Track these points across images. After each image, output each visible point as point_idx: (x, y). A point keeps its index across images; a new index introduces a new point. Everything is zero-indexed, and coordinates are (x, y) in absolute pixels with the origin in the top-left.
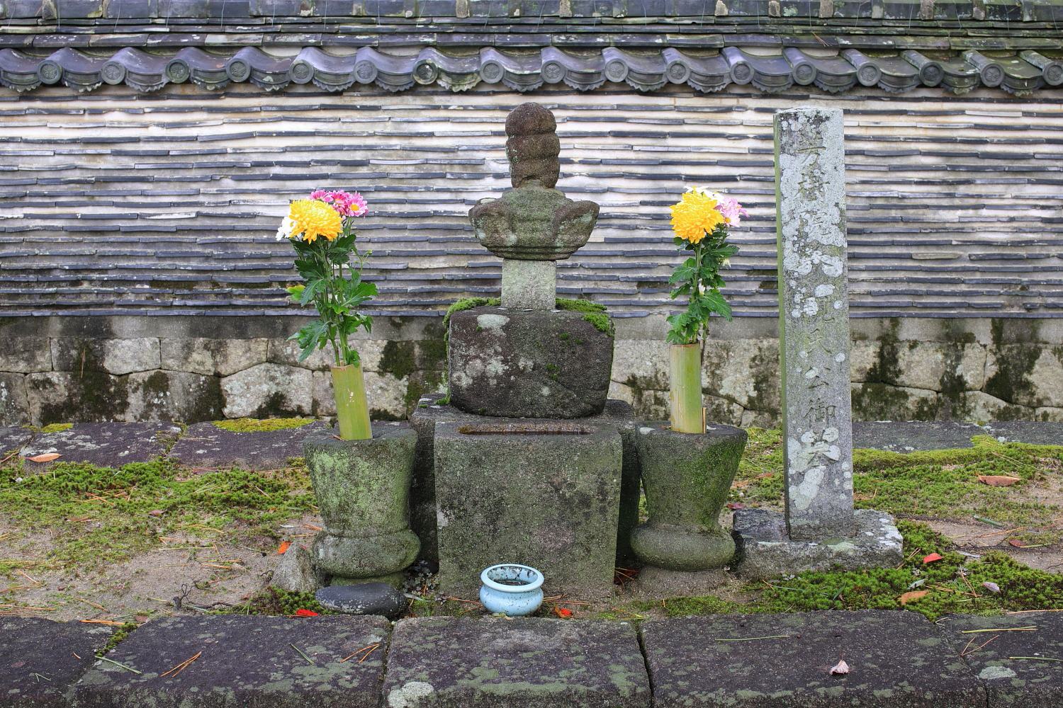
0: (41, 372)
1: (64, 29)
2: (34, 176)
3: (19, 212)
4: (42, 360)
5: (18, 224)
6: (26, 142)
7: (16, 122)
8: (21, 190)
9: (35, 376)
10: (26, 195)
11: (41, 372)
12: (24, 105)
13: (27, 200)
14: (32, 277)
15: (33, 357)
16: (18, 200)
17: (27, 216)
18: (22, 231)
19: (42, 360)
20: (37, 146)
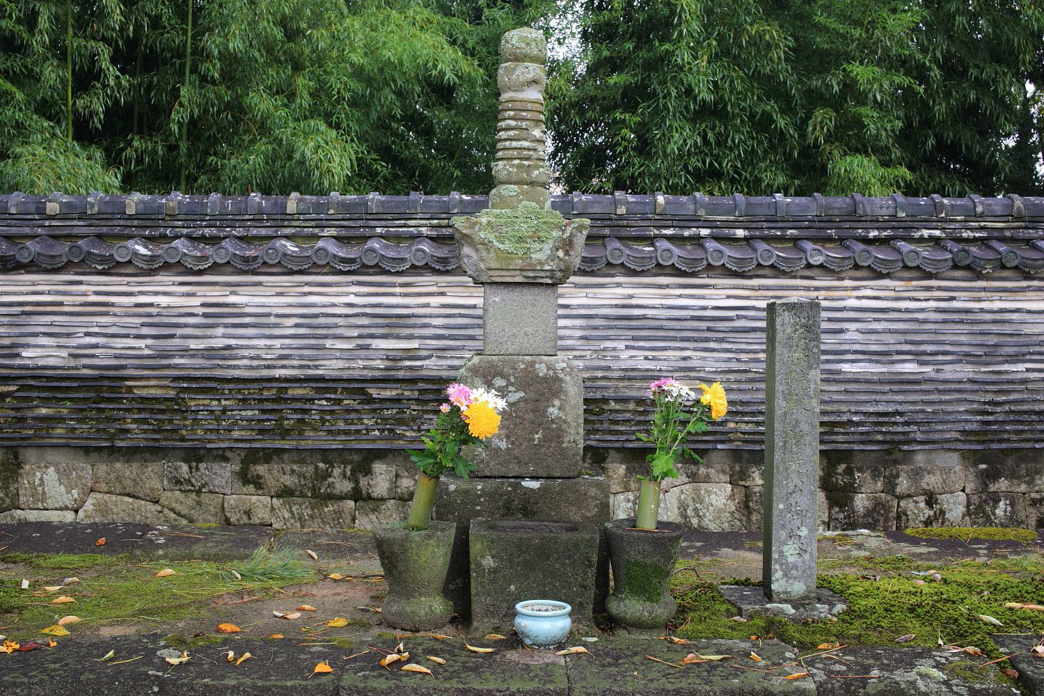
0: (1037, 492)
1: (1031, 225)
2: (1035, 338)
3: (1021, 367)
4: (1040, 482)
5: (1019, 376)
6: (1029, 312)
7: (1020, 296)
8: (1025, 349)
9: (1033, 495)
10: (1030, 353)
11: (1037, 492)
12: (1025, 284)
13: (1028, 357)
14: (1034, 417)
15: (1033, 480)
16: (1021, 358)
17: (1028, 370)
18: (1024, 381)
19: (1040, 482)
20: (1036, 316)
